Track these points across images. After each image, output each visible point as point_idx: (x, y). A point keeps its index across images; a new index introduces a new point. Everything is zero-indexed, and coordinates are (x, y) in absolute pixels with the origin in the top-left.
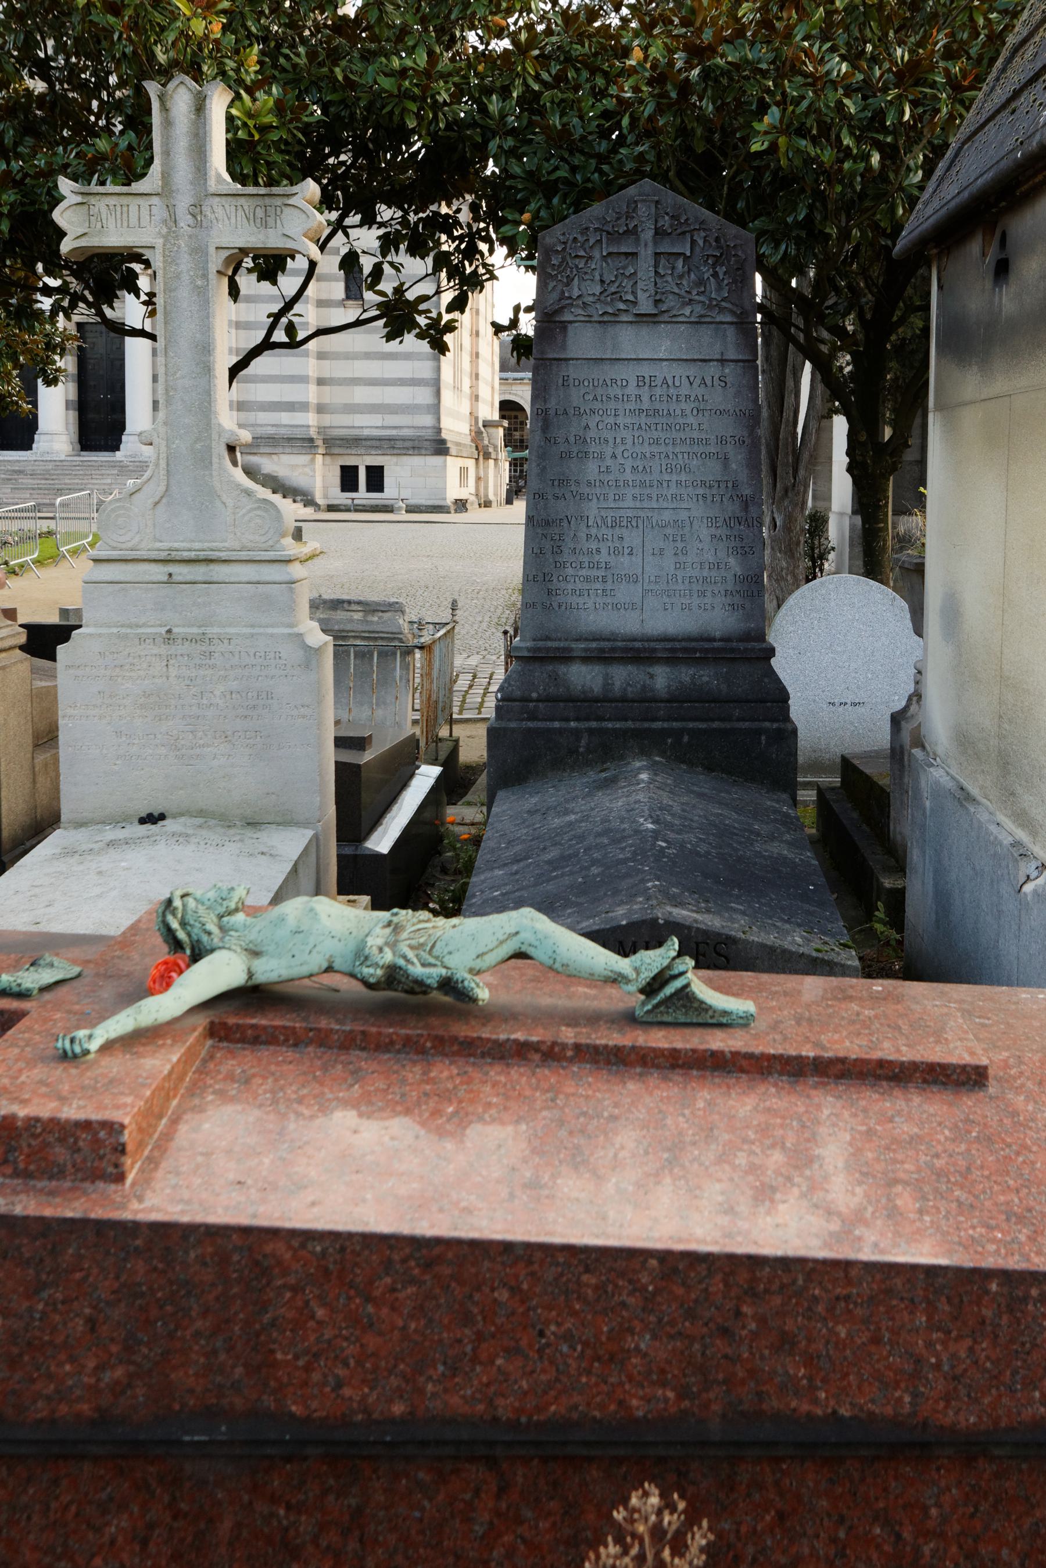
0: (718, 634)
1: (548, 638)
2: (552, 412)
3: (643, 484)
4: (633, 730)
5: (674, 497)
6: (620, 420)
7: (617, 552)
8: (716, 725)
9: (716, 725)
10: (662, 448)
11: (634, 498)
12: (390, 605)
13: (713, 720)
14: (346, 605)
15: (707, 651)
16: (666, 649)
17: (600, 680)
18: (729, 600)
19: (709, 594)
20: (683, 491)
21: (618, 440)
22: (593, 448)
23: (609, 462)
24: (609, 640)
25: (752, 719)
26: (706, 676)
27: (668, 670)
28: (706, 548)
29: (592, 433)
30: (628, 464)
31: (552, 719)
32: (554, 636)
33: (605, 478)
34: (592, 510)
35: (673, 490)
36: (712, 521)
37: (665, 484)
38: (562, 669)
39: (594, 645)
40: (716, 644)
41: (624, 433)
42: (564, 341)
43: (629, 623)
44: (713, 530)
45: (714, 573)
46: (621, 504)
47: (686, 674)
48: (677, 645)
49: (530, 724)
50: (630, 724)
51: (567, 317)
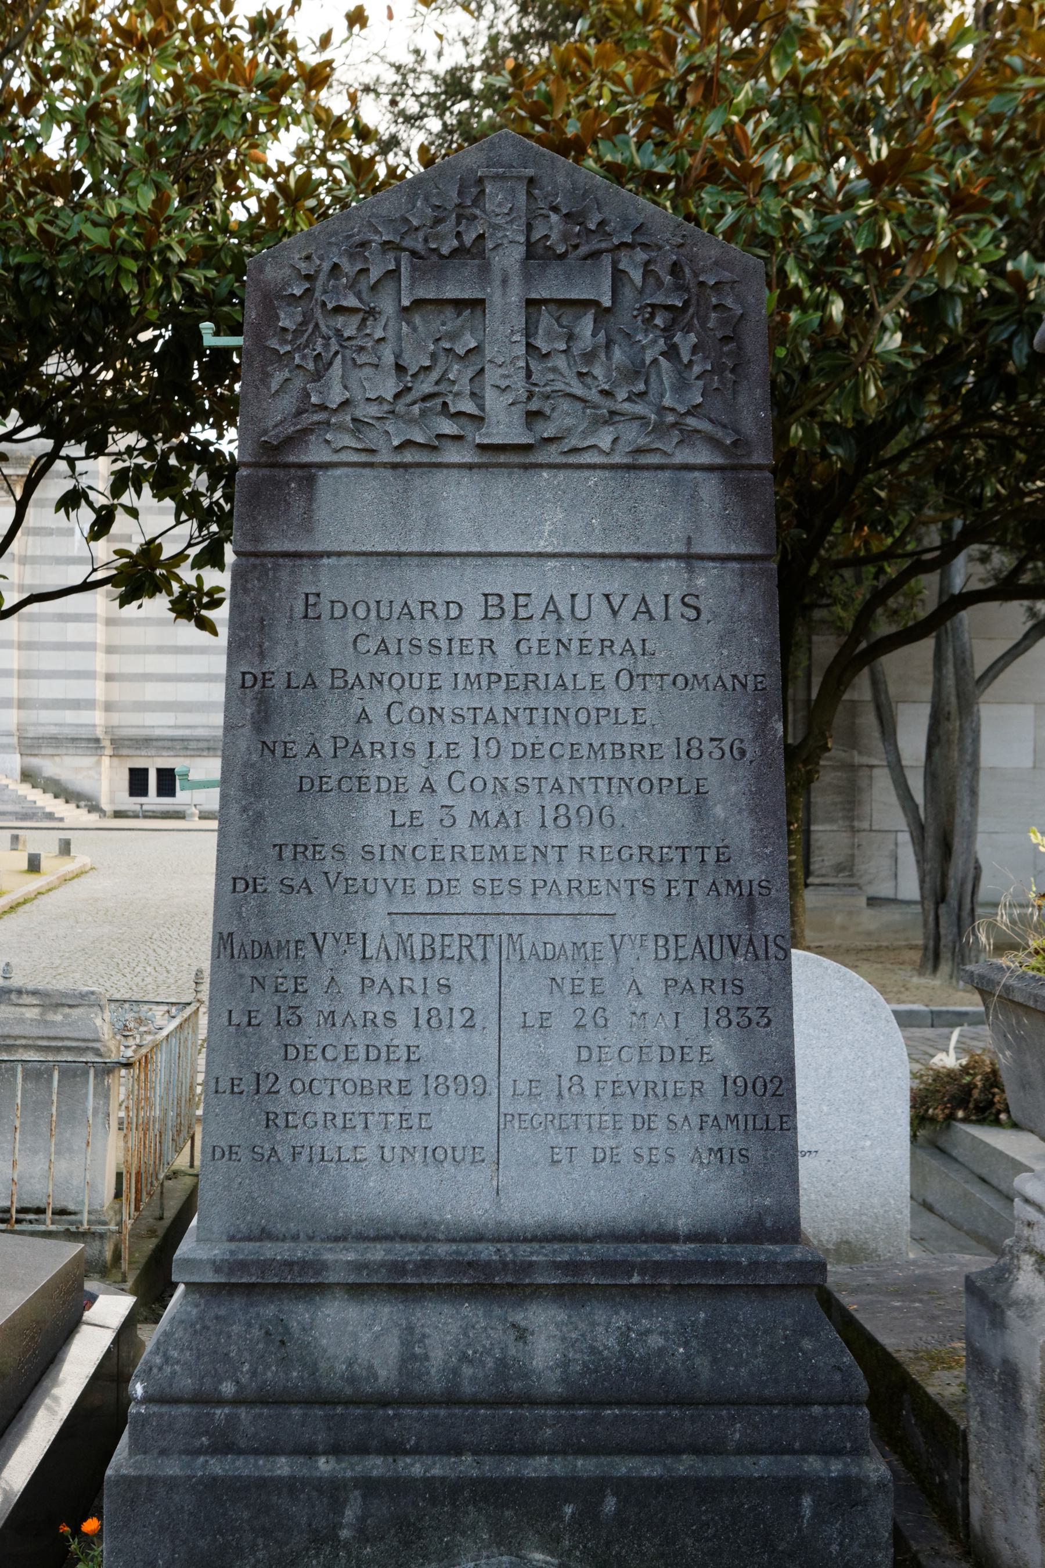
0: (683, 1224)
1: (265, 1235)
2: (278, 682)
3: (498, 855)
4: (481, 1480)
5: (574, 887)
6: (443, 701)
7: (433, 1021)
8: (685, 1465)
9: (685, 1465)
10: (546, 769)
11: (478, 888)
12: (82, 996)
13: (676, 1451)
14: (13, 996)
15: (658, 1268)
16: (557, 1266)
17: (392, 1346)
18: (709, 1139)
19: (659, 1124)
20: (596, 871)
21: (439, 749)
22: (376, 768)
23: (416, 802)
24: (414, 1239)
25: (776, 1450)
26: (654, 1334)
27: (562, 1316)
28: (653, 1011)
29: (376, 732)
30: (463, 807)
31: (271, 1450)
32: (280, 1228)
33: (407, 840)
34: (375, 917)
35: (572, 869)
36: (668, 944)
37: (552, 856)
38: (298, 1314)
39: (378, 1253)
40: (681, 1250)
41: (452, 732)
42: (309, 511)
43: (464, 1197)
44: (670, 968)
45: (673, 1073)
46: (446, 905)
47: (607, 1328)
48: (585, 1253)
49: (217, 1466)
50: (467, 1465)
51: (315, 453)
